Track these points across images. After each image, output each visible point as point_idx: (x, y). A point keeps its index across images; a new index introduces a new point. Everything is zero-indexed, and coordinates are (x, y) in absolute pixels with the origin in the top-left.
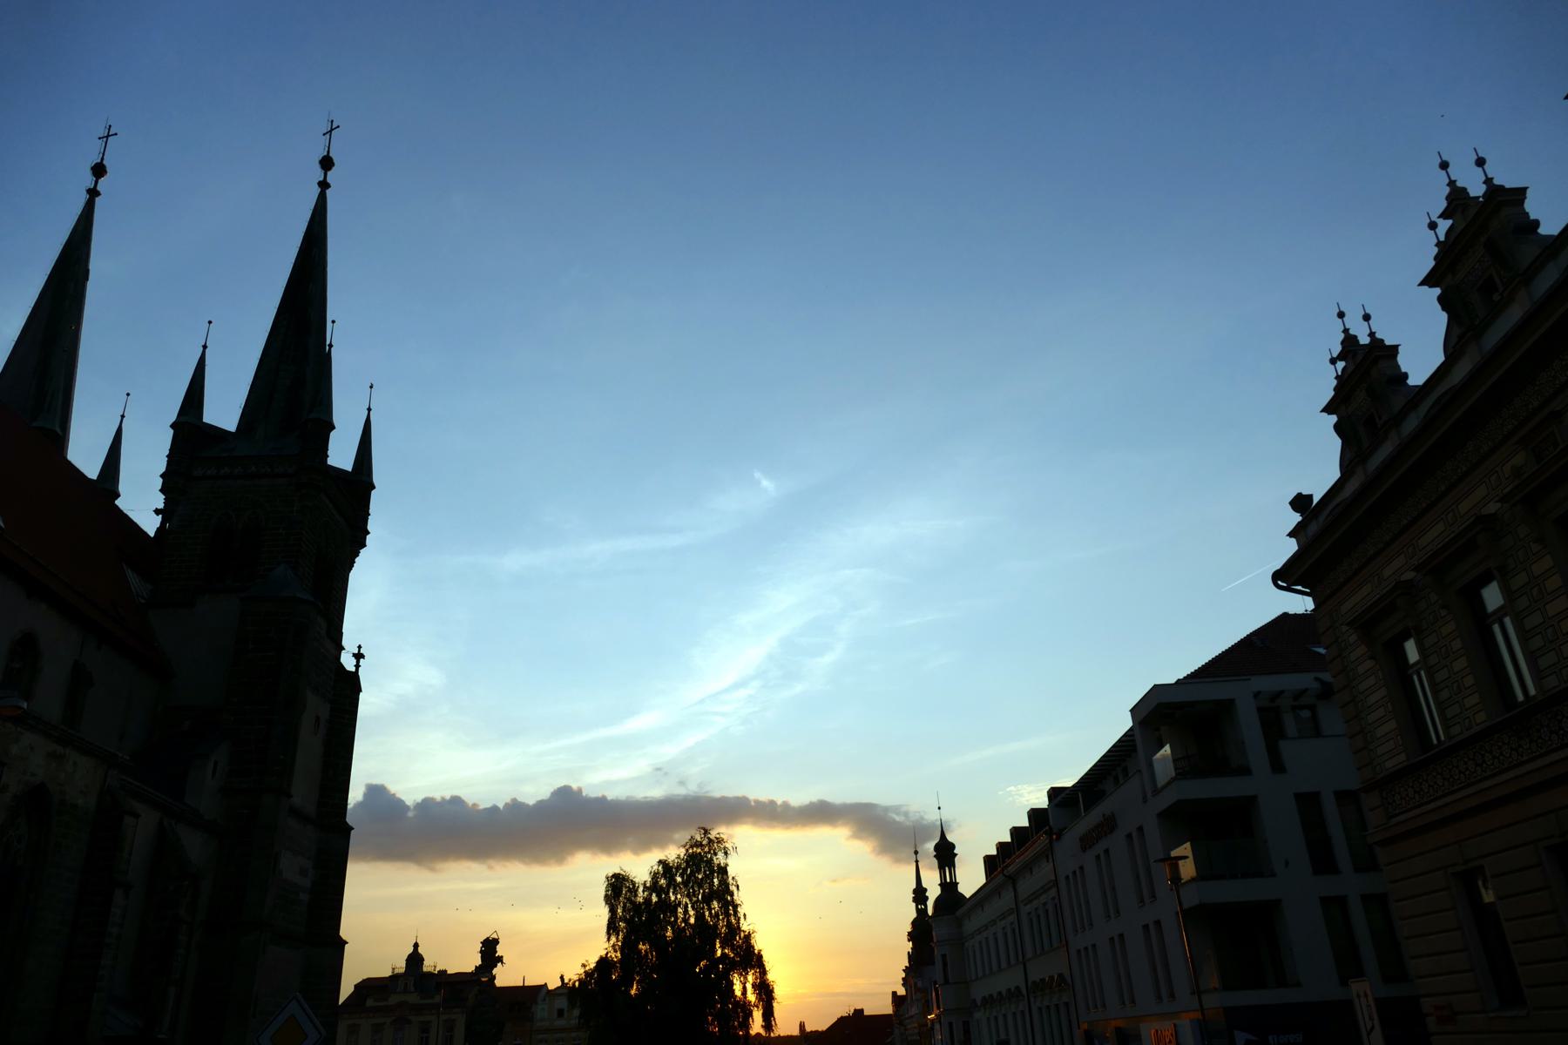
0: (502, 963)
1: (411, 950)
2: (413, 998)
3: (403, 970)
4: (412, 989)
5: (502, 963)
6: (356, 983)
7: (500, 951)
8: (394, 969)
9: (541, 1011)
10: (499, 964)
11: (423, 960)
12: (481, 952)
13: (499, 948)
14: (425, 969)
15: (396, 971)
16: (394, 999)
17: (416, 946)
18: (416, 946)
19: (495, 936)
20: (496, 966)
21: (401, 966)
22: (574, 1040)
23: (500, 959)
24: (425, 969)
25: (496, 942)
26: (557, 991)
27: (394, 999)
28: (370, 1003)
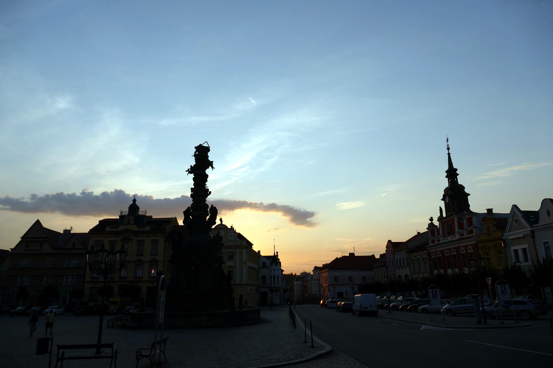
0: (212, 167)
2: (134, 228)
4: (133, 223)
5: (212, 167)
6: (100, 220)
7: (211, 157)
8: (121, 212)
10: (210, 167)
11: (139, 208)
12: (195, 155)
13: (209, 154)
14: (140, 213)
15: (123, 214)
16: (121, 228)
19: (206, 145)
20: (208, 168)
22: (230, 254)
23: (210, 164)
24: (140, 213)
25: (207, 149)
26: (217, 227)
27: (121, 228)
28: (108, 229)
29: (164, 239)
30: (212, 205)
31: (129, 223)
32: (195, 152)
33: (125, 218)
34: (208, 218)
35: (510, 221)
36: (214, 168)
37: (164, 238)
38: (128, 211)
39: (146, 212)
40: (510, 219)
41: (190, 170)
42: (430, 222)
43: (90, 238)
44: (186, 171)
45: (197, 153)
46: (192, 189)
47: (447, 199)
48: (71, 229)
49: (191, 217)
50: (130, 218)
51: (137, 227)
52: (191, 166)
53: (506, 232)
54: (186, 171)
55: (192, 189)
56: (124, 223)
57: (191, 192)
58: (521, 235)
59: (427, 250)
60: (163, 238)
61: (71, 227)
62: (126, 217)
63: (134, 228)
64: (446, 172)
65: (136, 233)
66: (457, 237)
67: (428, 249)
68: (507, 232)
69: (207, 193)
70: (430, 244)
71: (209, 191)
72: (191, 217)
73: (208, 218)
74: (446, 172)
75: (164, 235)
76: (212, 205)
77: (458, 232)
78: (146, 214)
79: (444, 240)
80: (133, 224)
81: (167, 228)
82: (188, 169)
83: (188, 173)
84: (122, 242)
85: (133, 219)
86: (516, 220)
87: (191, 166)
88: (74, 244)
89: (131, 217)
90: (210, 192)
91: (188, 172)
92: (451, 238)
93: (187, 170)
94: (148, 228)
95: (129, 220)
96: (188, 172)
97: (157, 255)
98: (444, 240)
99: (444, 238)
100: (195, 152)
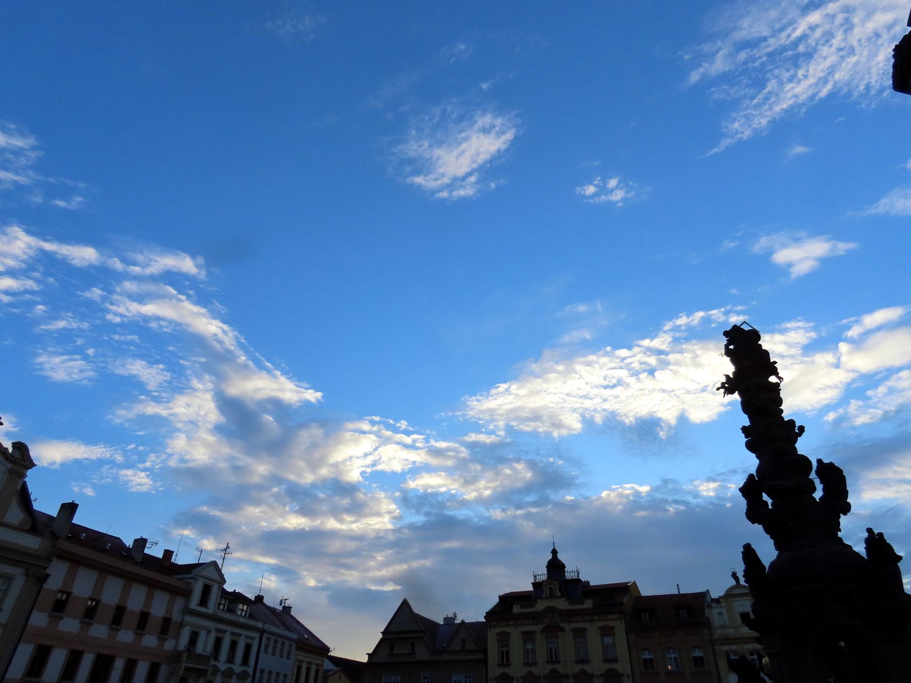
1: (550, 556)
2: (562, 604)
3: (545, 578)
4: (559, 594)
6: (502, 593)
8: (535, 577)
9: (716, 616)
11: (563, 566)
14: (568, 576)
15: (539, 579)
16: (540, 606)
17: (554, 552)
18: (554, 552)
21: (542, 573)
24: (568, 576)
25: (755, 336)
27: (540, 606)
28: (516, 609)
29: (624, 624)
30: (819, 461)
31: (552, 596)
32: (725, 345)
33: (544, 587)
34: (818, 495)
36: (782, 379)
37: (623, 621)
38: (545, 572)
39: (578, 573)
41: (727, 385)
43: (488, 629)
44: (718, 389)
45: (732, 347)
46: (745, 430)
48: (455, 616)
49: (765, 497)
50: (553, 586)
51: (567, 603)
52: (727, 376)
54: (718, 389)
55: (745, 430)
56: (544, 596)
57: (746, 437)
60: (621, 623)
61: (455, 614)
62: (545, 583)
63: (562, 604)
65: (569, 615)
69: (792, 431)
71: (797, 425)
72: (765, 497)
73: (818, 495)
75: (623, 615)
76: (819, 461)
78: (578, 576)
80: (558, 597)
81: (624, 601)
82: (723, 384)
83: (725, 393)
84: (545, 634)
85: (557, 586)
87: (727, 376)
88: (463, 641)
89: (555, 582)
90: (802, 429)
91: (722, 390)
93: (719, 386)
94: (588, 604)
95: (551, 589)
96: (722, 390)
97: (615, 661)
100: (727, 346)
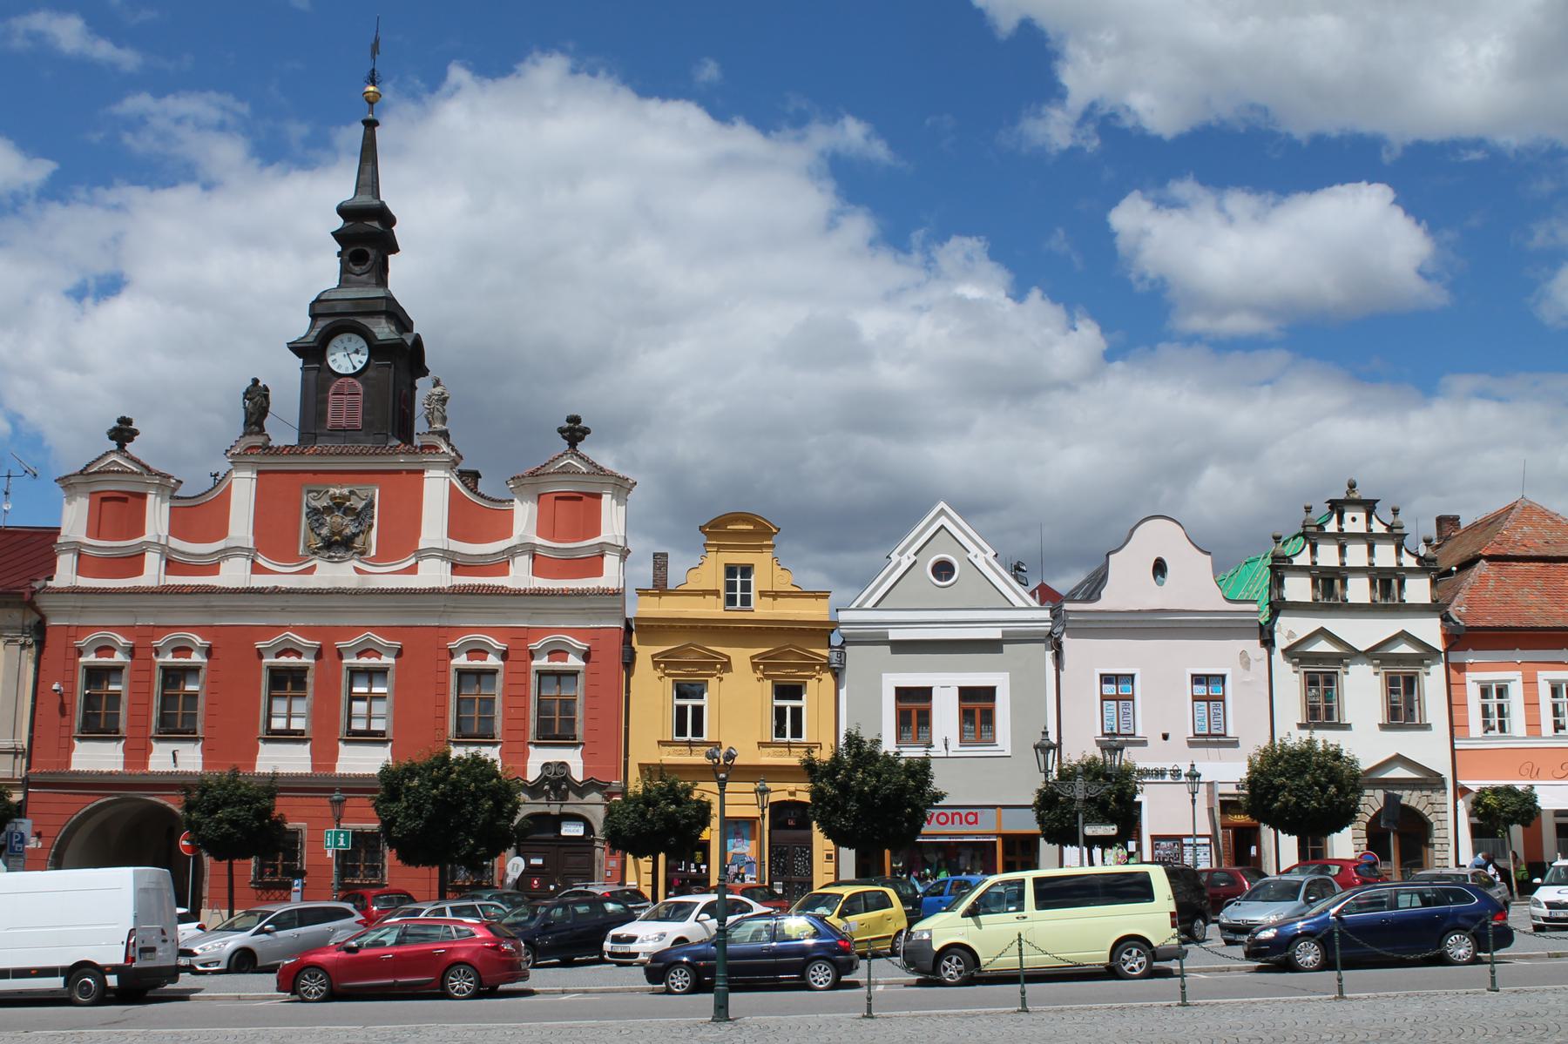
35: (899, 564)
40: (901, 553)
42: (113, 445)
47: (346, 359)
53: (859, 608)
58: (995, 633)
59: (37, 610)
64: (343, 211)
66: (433, 574)
67: (44, 602)
68: (869, 604)
70: (65, 573)
74: (343, 211)
77: (446, 555)
79: (257, 569)
86: (943, 570)
92: (358, 570)
98: (257, 569)
99: (261, 561)
